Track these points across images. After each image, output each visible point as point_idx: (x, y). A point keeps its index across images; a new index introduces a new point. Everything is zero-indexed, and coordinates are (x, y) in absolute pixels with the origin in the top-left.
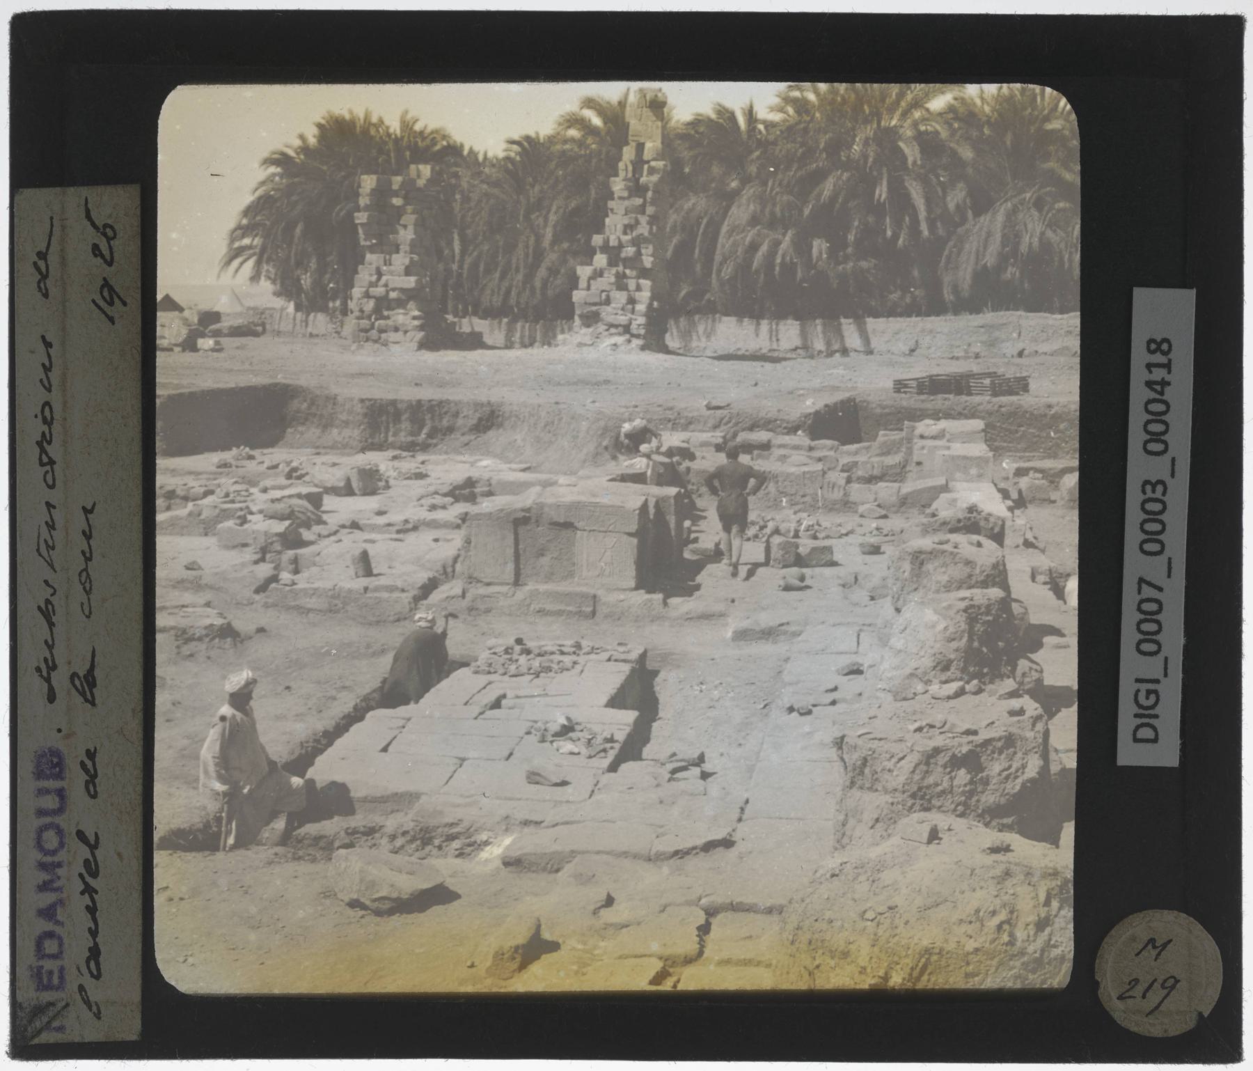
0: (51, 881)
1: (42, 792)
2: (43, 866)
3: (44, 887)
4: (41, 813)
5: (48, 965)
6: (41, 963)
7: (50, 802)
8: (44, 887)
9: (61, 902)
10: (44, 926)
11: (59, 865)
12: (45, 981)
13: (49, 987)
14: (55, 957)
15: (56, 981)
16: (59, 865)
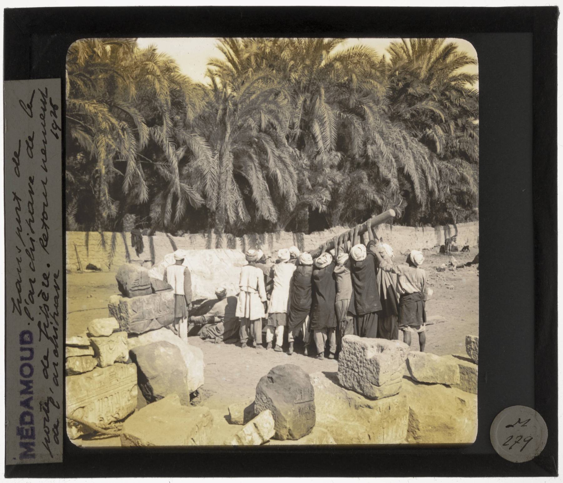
0: (26, 389)
1: (22, 349)
2: (22, 382)
3: (22, 392)
4: (22, 359)
5: (27, 427)
6: (23, 426)
7: (27, 354)
8: (22, 392)
9: (31, 399)
10: (24, 409)
11: (31, 382)
12: (25, 434)
13: (27, 437)
14: (27, 423)
15: (30, 433)
16: (31, 382)
